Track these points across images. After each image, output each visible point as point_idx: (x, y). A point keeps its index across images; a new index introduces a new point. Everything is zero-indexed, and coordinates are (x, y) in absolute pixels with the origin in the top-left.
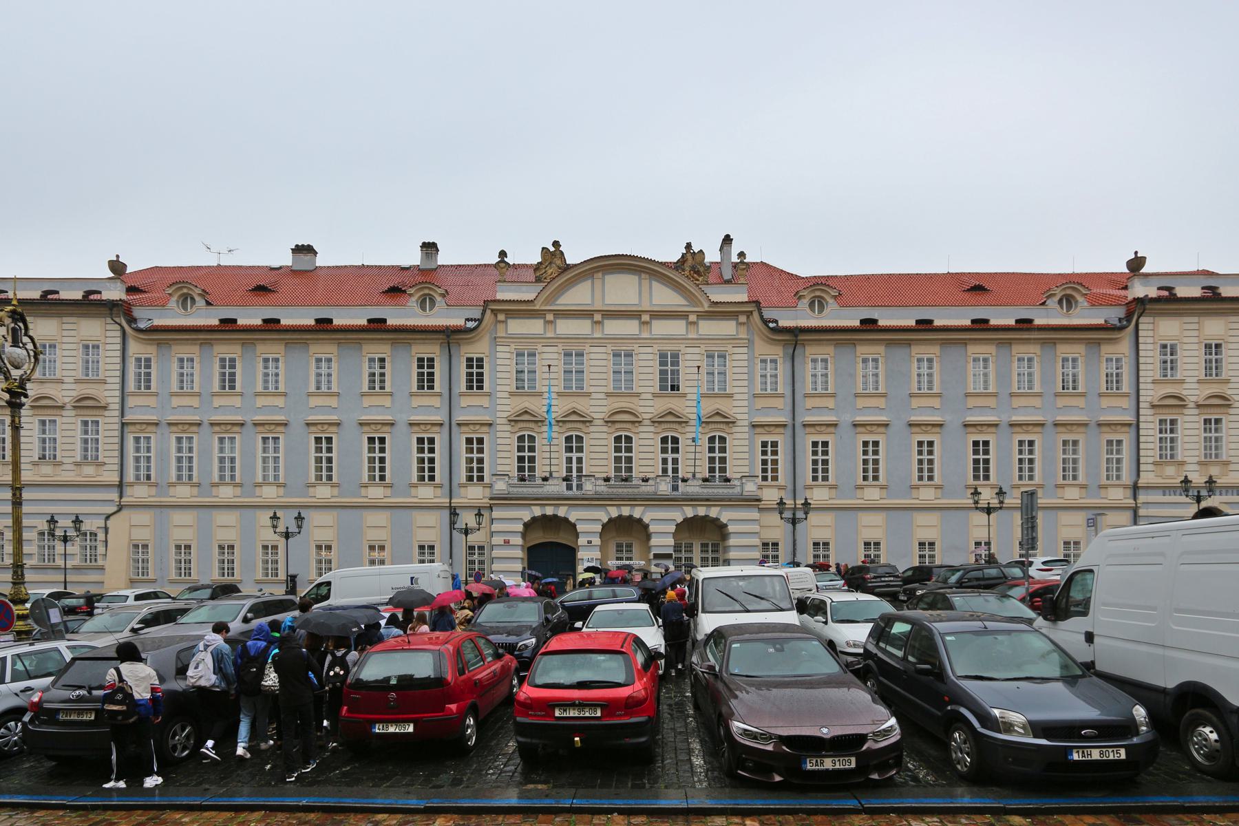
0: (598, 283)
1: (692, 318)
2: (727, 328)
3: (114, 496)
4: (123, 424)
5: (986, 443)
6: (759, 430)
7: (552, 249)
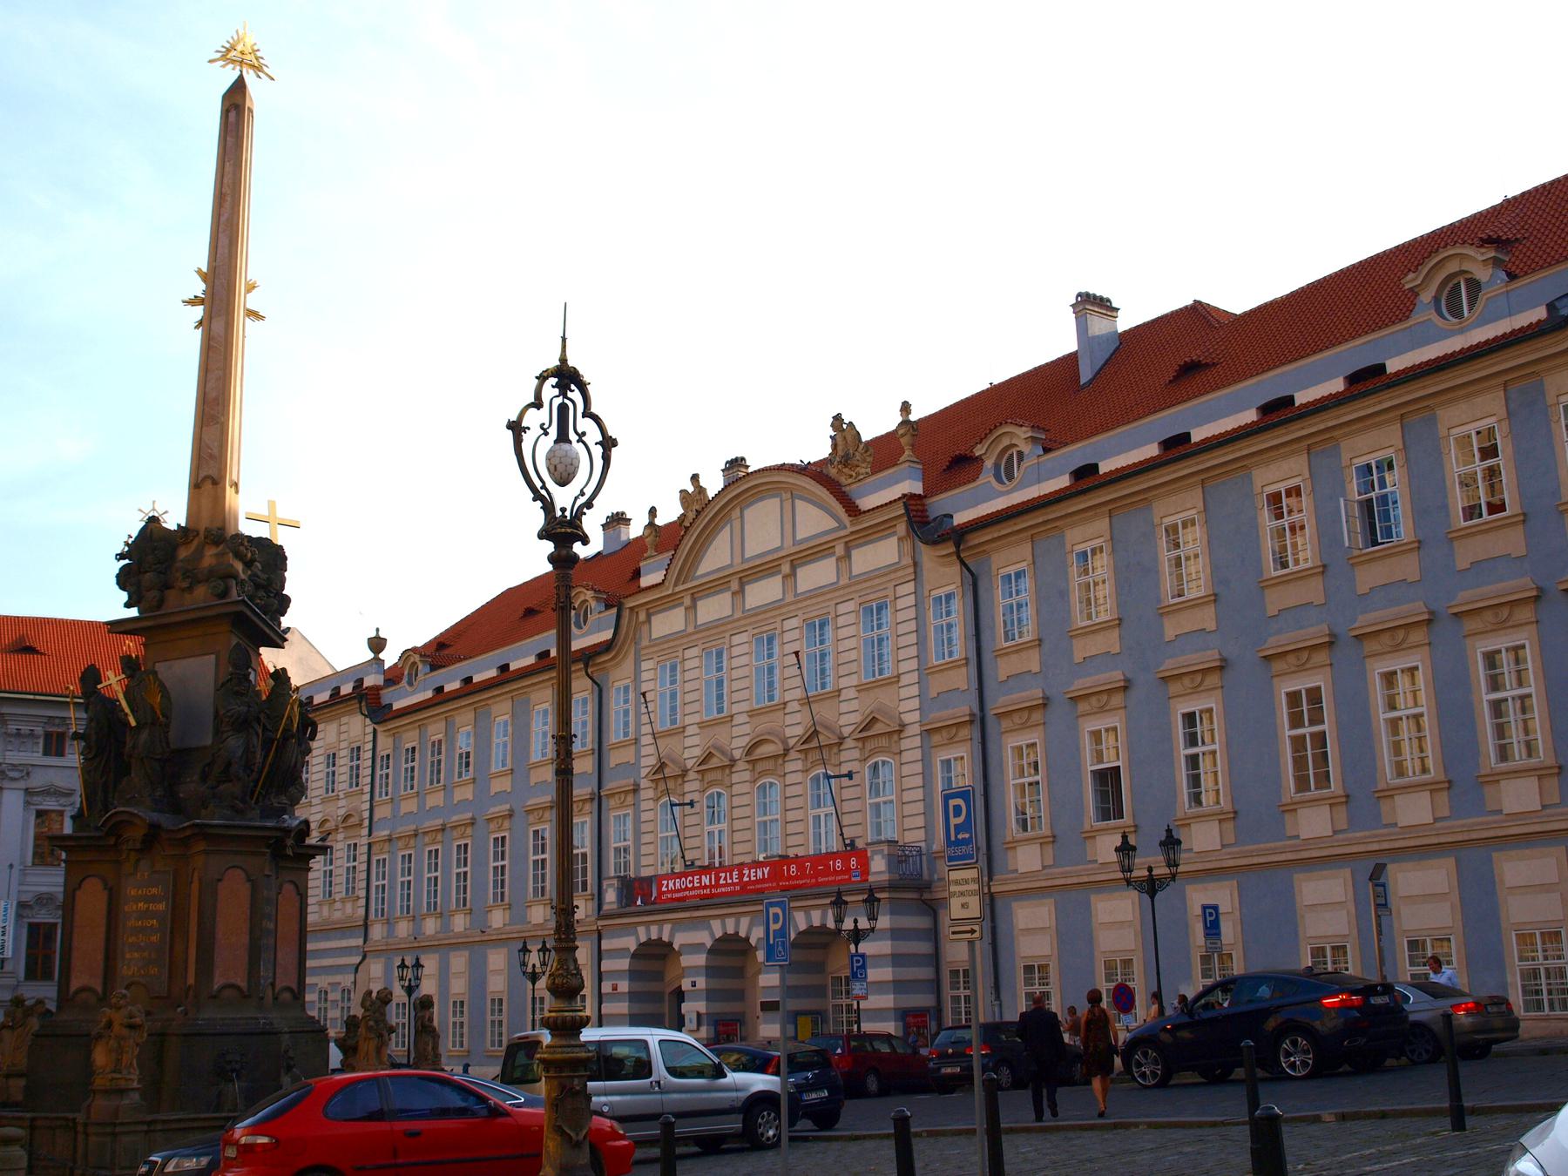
0: (737, 524)
2: (884, 552)
3: (360, 941)
4: (370, 845)
5: (1315, 695)
6: (936, 738)
7: (691, 489)
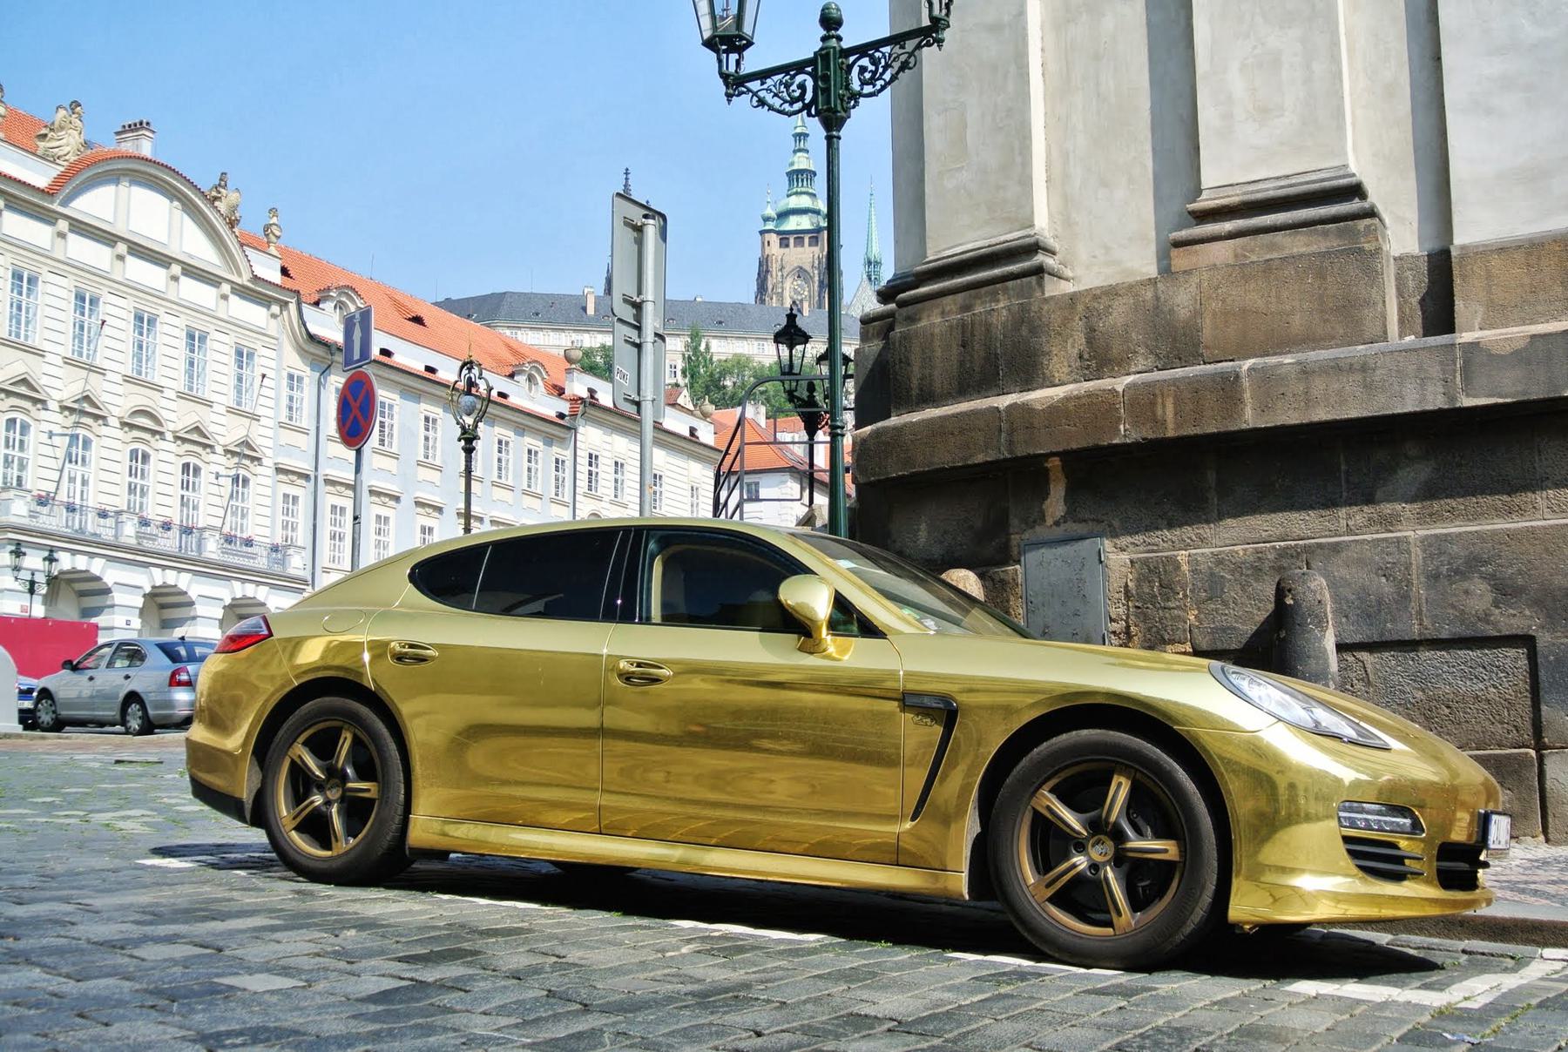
1: (226, 288)
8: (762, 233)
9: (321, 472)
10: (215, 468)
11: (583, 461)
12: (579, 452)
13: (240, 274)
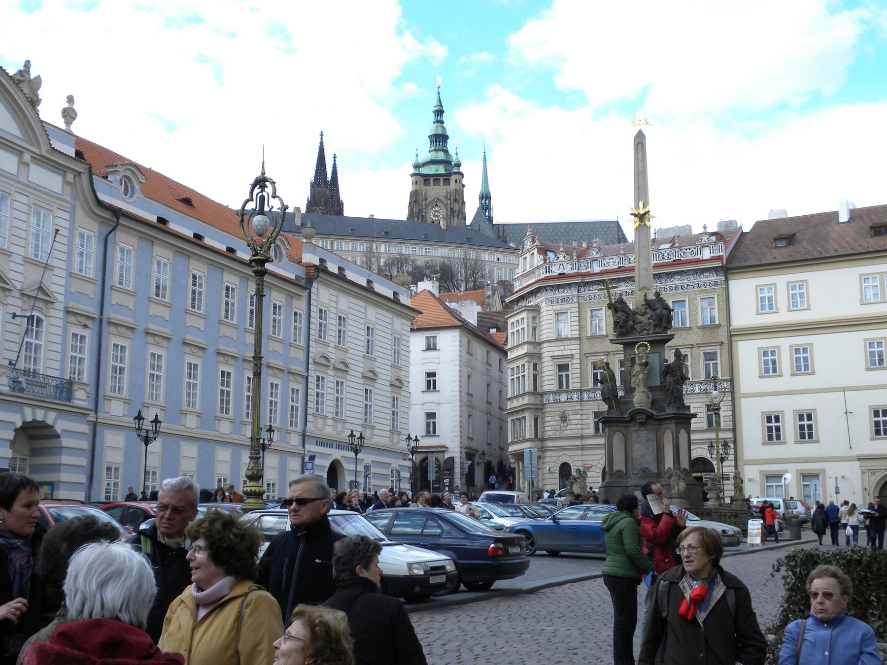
1: (27, 157)
6: (72, 318)
8: (412, 175)
9: (105, 316)
10: (12, 310)
11: (315, 314)
12: (312, 308)
13: (39, 147)
